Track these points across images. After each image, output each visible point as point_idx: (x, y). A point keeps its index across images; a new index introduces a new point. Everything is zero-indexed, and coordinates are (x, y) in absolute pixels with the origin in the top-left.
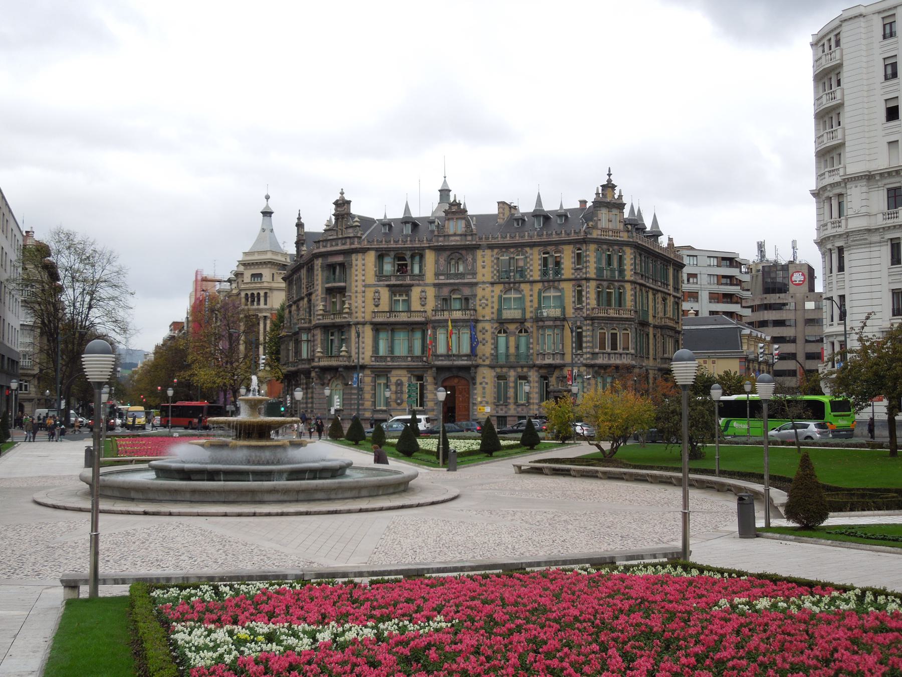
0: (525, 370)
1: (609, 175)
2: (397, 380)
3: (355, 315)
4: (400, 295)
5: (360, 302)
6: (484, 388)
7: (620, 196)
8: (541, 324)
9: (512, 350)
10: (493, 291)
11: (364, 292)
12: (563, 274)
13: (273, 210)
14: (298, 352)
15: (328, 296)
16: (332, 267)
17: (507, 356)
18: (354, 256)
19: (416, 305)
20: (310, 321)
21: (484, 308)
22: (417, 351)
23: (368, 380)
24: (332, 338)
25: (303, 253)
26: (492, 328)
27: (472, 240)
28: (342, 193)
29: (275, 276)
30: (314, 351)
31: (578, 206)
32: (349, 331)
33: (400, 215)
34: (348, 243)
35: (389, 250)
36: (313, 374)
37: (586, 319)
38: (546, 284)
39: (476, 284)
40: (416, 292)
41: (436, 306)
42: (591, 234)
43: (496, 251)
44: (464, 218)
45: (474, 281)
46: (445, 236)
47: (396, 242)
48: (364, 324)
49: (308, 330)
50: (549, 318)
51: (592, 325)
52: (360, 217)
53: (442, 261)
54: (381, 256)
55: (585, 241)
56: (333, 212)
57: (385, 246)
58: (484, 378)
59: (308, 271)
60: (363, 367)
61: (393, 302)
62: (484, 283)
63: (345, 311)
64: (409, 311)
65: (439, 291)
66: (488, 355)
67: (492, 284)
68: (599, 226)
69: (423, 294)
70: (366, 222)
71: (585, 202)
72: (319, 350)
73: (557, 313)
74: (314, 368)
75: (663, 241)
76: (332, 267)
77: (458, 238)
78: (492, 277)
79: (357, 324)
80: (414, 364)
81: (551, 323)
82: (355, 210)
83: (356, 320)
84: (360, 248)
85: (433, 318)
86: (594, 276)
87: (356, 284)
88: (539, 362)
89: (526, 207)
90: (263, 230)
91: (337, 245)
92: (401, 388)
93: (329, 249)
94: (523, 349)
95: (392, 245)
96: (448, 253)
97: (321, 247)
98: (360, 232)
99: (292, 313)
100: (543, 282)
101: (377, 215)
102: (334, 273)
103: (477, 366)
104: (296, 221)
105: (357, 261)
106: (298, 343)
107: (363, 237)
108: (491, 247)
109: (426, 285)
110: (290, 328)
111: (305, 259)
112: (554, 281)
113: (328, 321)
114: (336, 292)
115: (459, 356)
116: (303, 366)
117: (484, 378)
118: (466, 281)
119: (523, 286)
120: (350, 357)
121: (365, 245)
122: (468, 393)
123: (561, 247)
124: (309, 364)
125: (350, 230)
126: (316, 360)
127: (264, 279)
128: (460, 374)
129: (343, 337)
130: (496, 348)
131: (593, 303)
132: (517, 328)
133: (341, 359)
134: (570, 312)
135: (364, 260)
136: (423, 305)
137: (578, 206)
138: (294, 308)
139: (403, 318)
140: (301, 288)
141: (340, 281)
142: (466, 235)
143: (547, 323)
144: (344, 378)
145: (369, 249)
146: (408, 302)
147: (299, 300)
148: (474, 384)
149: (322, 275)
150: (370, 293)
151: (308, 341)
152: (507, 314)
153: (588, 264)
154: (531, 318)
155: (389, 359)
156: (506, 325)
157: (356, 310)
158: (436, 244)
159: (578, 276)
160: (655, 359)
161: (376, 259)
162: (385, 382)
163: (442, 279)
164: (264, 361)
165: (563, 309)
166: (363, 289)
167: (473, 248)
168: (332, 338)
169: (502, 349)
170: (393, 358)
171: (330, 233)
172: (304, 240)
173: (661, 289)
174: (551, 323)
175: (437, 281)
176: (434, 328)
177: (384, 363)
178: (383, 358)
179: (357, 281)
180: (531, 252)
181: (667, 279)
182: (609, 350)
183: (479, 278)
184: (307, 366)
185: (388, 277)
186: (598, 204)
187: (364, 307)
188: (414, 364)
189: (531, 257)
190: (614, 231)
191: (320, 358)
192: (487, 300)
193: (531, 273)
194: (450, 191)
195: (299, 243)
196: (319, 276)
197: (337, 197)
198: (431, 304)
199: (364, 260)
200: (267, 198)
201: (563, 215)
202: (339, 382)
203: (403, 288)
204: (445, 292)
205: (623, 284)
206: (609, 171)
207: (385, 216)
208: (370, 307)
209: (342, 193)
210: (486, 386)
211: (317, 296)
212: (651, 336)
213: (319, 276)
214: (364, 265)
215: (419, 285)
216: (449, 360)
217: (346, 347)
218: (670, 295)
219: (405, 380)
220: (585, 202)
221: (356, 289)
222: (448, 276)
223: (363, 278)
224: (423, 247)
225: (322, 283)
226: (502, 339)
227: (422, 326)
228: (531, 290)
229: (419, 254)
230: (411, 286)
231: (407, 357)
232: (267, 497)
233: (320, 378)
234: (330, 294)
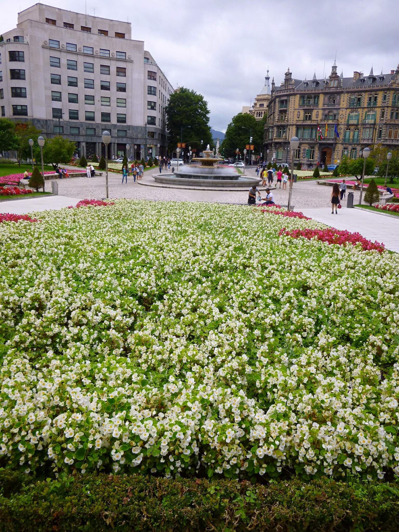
9: (351, 137)
16: (282, 102)
19: (314, 118)
31: (390, 73)
33: (311, 79)
39: (340, 109)
40: (314, 113)
48: (293, 125)
50: (368, 124)
52: (295, 80)
53: (326, 99)
55: (389, 89)
67: (346, 109)
70: (298, 82)
73: (372, 122)
79: (290, 125)
82: (293, 77)
86: (390, 105)
88: (362, 142)
94: (356, 137)
95: (307, 92)
96: (329, 95)
101: (303, 79)
103: (336, 144)
105: (292, 98)
108: (348, 92)
113: (279, 124)
114: (284, 112)
119: (359, 110)
121: (296, 92)
123: (378, 92)
130: (345, 136)
131: (389, 117)
134: (378, 121)
137: (390, 73)
139: (308, 123)
143: (367, 126)
145: (297, 94)
150: (296, 113)
152: (351, 122)
163: (326, 107)
167: (340, 93)
182: (392, 138)
183: (341, 106)
195: (272, 91)
196: (277, 104)
197: (287, 71)
198: (320, 117)
200: (268, 71)
201: (382, 78)
204: (327, 112)
208: (296, 118)
213: (277, 104)
222: (328, 105)
226: (348, 133)
227: (317, 126)
229: (316, 96)
233: (275, 146)
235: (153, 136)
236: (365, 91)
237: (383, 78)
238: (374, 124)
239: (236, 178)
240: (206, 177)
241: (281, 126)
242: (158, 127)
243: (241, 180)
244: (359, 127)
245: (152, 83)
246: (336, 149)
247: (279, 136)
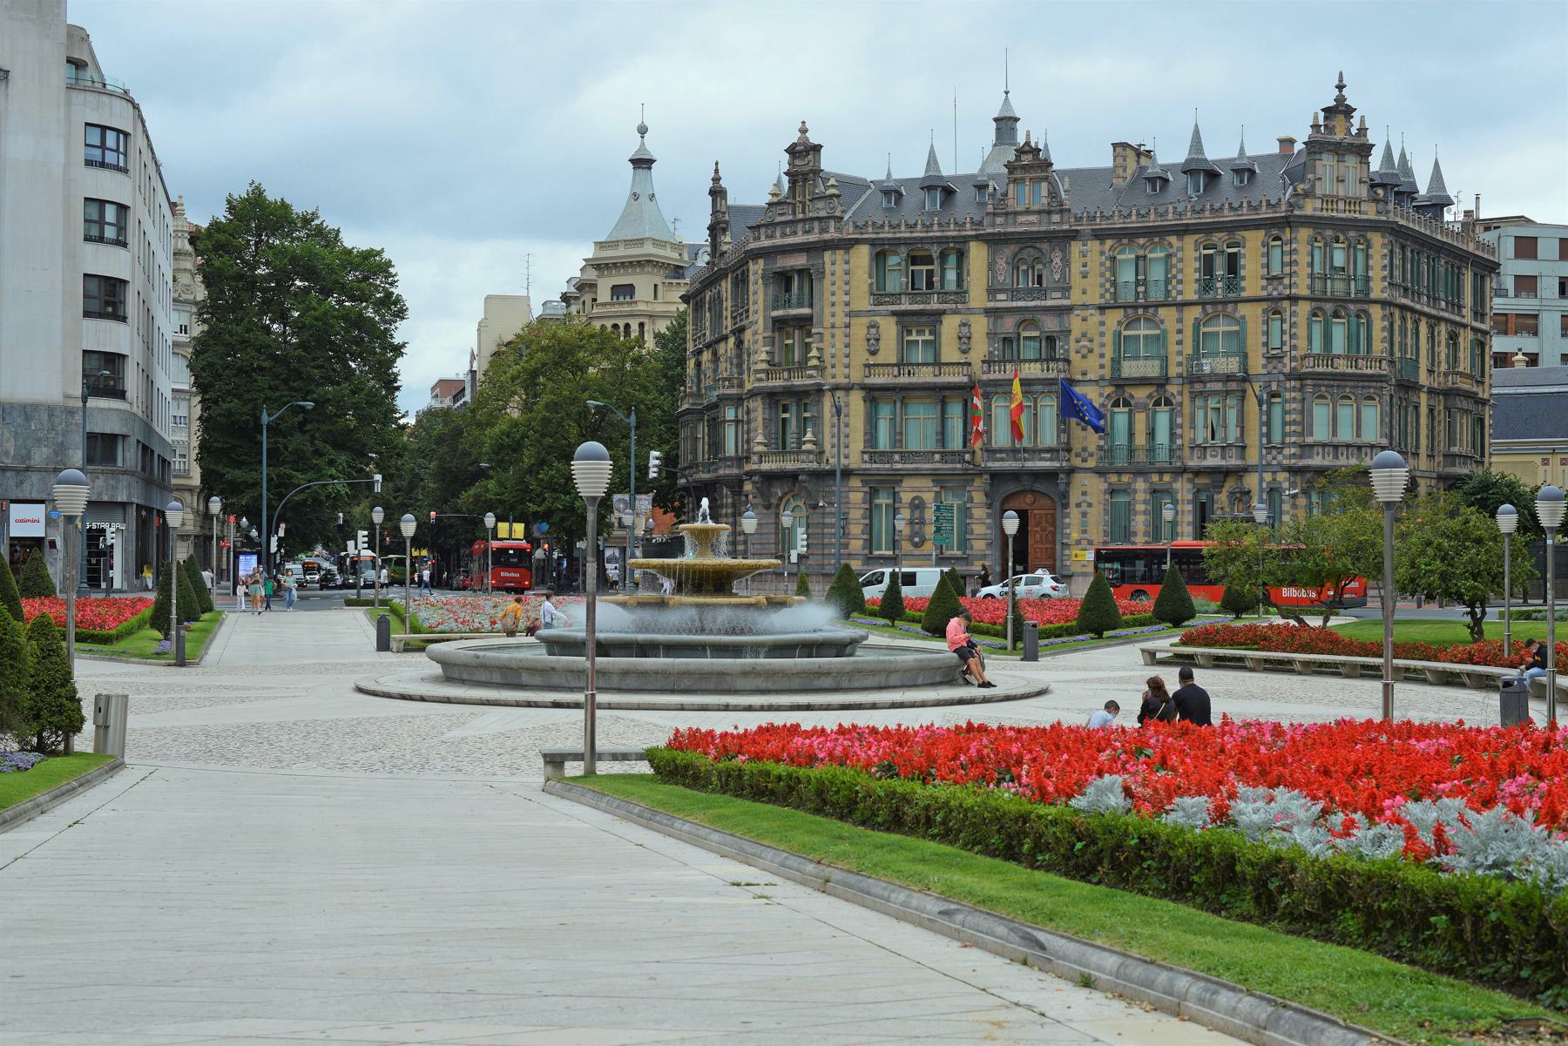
0: (1167, 478)
1: (1340, 87)
2: (914, 498)
3: (829, 371)
4: (920, 332)
5: (840, 345)
6: (1084, 515)
7: (1363, 131)
8: (1198, 387)
9: (1140, 439)
10: (1102, 324)
11: (848, 326)
12: (1243, 289)
13: (655, 156)
14: (716, 445)
15: (777, 334)
16: (784, 279)
17: (1131, 451)
18: (828, 256)
19: (950, 353)
20: (741, 385)
21: (1084, 357)
22: (956, 443)
23: (857, 497)
24: (785, 415)
25: (725, 248)
26: (1101, 395)
27: (1061, 223)
28: (804, 131)
29: (660, 288)
30: (748, 442)
31: (1275, 149)
32: (819, 402)
33: (920, 173)
34: (816, 230)
35: (897, 243)
36: (748, 487)
37: (1290, 376)
38: (1209, 308)
39: (1070, 309)
40: (950, 325)
41: (990, 353)
42: (1301, 208)
43: (1109, 243)
44: (1046, 179)
45: (1065, 302)
46: (1007, 214)
47: (911, 227)
48: (848, 389)
49: (738, 401)
50: (1215, 377)
51: (1301, 389)
52: (836, 176)
53: (1001, 264)
54: (880, 257)
55: (1288, 222)
56: (786, 167)
57: (890, 236)
58: (1084, 494)
59: (736, 284)
60: (847, 473)
61: (905, 346)
62: (1085, 306)
63: (810, 364)
64: (937, 363)
65: (995, 322)
66: (1092, 448)
67: (1102, 309)
68: (1318, 192)
69: (965, 330)
70: (853, 186)
71: (1291, 142)
72: (760, 439)
73: (1232, 365)
74: (750, 474)
76: (784, 279)
77: (1032, 218)
78: (1102, 296)
79: (835, 388)
80: (946, 466)
81: (1218, 386)
82: (829, 163)
83: (833, 381)
84: (840, 240)
85: (985, 377)
86: (1306, 292)
87: (833, 309)
88: (1194, 462)
90: (635, 196)
91: (795, 233)
92: (922, 513)
93: (778, 241)
95: (904, 234)
96: (1014, 248)
97: (763, 237)
98: (840, 208)
99: (703, 367)
100: (1203, 304)
102: (788, 289)
103: (1071, 471)
104: (710, 184)
106: (716, 425)
107: (846, 217)
108: (1100, 236)
109: (970, 311)
110: (699, 395)
111: (730, 260)
112: (1225, 303)
113: (777, 383)
115: (1035, 452)
116: (728, 471)
117: (1084, 494)
118: (1049, 303)
119: (1162, 312)
120: (822, 453)
121: (849, 232)
122: (1054, 524)
124: (740, 466)
125: (820, 204)
126: (755, 458)
127: (637, 297)
128: (1038, 487)
129: (807, 415)
132: (1150, 396)
133: (803, 457)
134: (1257, 364)
135: (847, 262)
136: (964, 352)
137: (1275, 149)
138: (706, 356)
139: (926, 376)
140: (721, 316)
141: (800, 305)
142: (1049, 213)
144: (809, 494)
145: (857, 242)
146: (934, 345)
147: (717, 342)
148: (1066, 506)
149: (766, 294)
150: (860, 328)
151: (737, 422)
152: (1130, 369)
153: (1294, 268)
154: (1180, 376)
155: (897, 457)
156: (1129, 390)
157: (834, 361)
158: (990, 230)
159: (1275, 293)
160: (1431, 456)
161: (871, 260)
162: (890, 501)
163: (1002, 301)
164: (657, 462)
166: (847, 320)
168: (785, 415)
170: (907, 456)
171: (779, 210)
172: (727, 223)
173: (1446, 315)
174: (1218, 386)
175: (991, 305)
176: (987, 396)
177: (887, 466)
178: (885, 456)
179: (833, 304)
180: (1180, 244)
181: (1458, 292)
183: (1076, 298)
184: (735, 471)
185: (896, 297)
186: (1315, 147)
187: (848, 356)
188: (946, 466)
189: (1180, 255)
190: (1349, 201)
191: (761, 455)
192: (1091, 341)
193: (1180, 287)
194: (1017, 120)
195: (715, 229)
196: (759, 294)
197: (794, 137)
198: (980, 349)
199: (847, 262)
200: (643, 130)
201: (1245, 172)
202: (801, 503)
203: (924, 319)
204: (1008, 325)
205: (1366, 306)
206: (1341, 79)
207: (889, 175)
208: (861, 356)
209: (804, 131)
210: (1088, 510)
211: (756, 333)
212: (1424, 410)
213: (759, 294)
214: (847, 273)
215: (956, 312)
216: (1016, 460)
217: (814, 434)
218: (1465, 326)
219: (928, 497)
220: (1291, 142)
221: (832, 320)
222: (1014, 293)
223: (846, 298)
224: (964, 237)
225: (765, 309)
227: (965, 391)
228: (1180, 321)
230: (940, 314)
231: (933, 453)
232: (741, 683)
234: (780, 329)
235: (110, 458)
237: (1252, 172)
239: (840, 648)
240: (736, 650)
241: (790, 392)
242: (135, 409)
243: (862, 657)
244: (1172, 389)
245: (110, 186)
246: (1074, 499)
247: (779, 445)
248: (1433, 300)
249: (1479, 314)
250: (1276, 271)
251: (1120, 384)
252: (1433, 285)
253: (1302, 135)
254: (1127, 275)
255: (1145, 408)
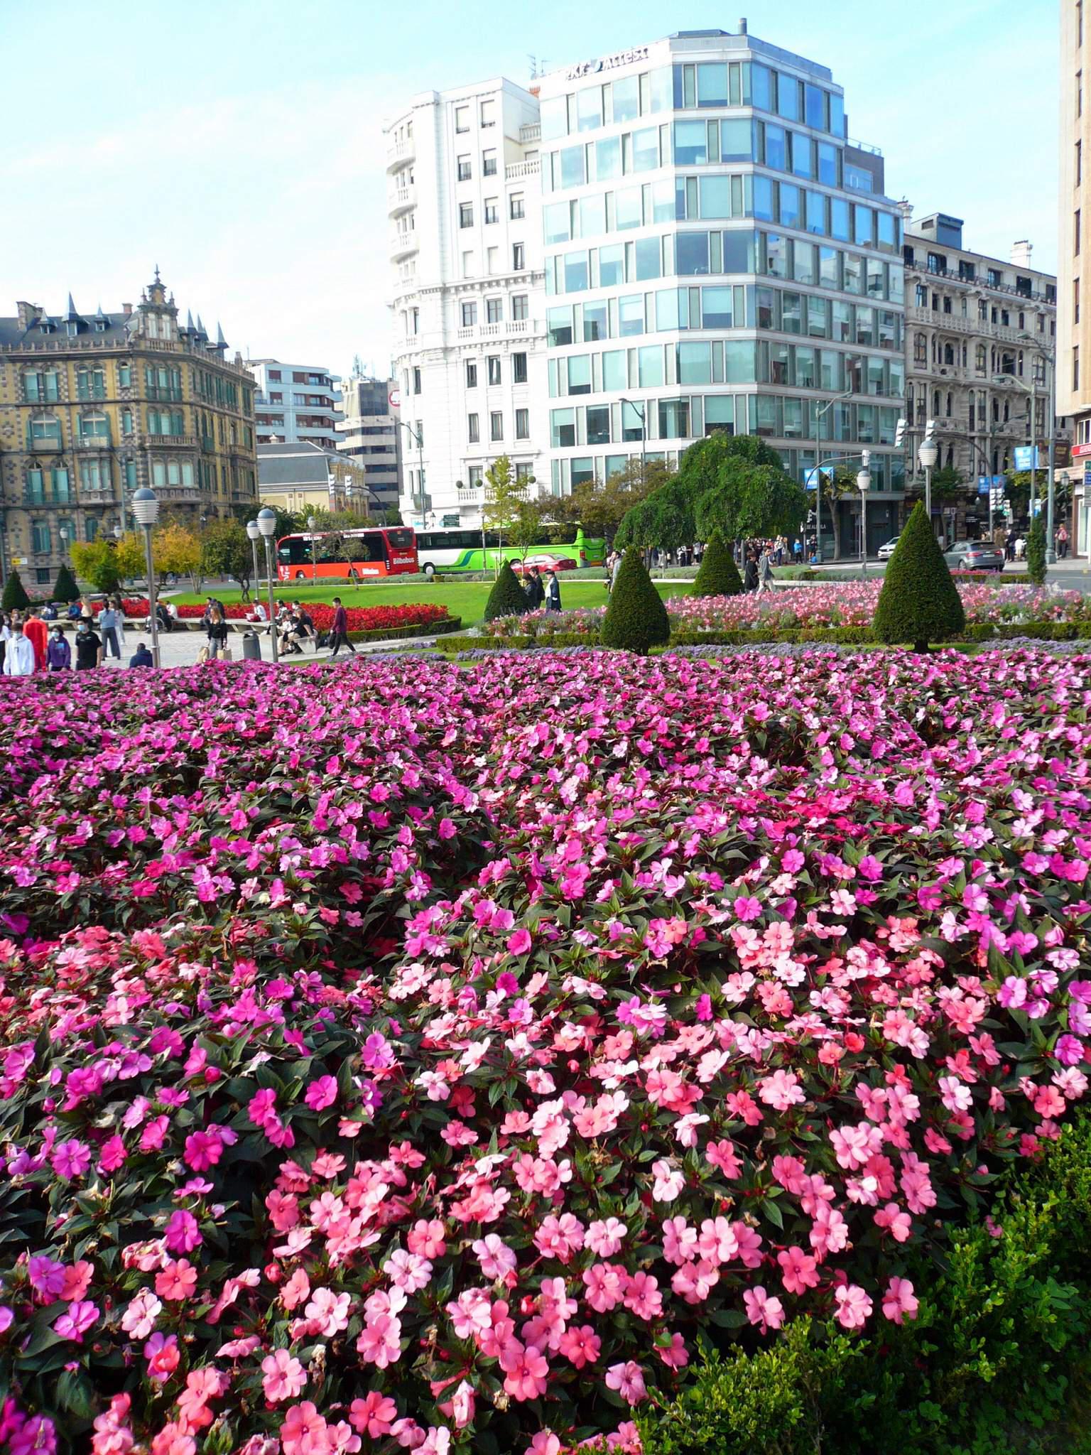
7: (172, 300)
8: (83, 456)
9: (49, 488)
17: (44, 496)
50: (92, 449)
67: (17, 406)
75: (229, 356)
81: (95, 455)
88: (83, 502)
89: (55, 309)
123: (101, 362)
137: (120, 310)
152: (41, 445)
156: (39, 459)
160: (225, 492)
165: (110, 436)
169: (37, 488)
174: (95, 455)
181: (235, 400)
186: (146, 308)
212: (219, 468)
226: (36, 476)
236: (68, 358)
238: (112, 449)
244: (67, 457)
246: (10, 526)
248: (221, 404)
249: (248, 413)
250: (127, 384)
251: (35, 454)
252: (219, 397)
253: (136, 302)
254: (33, 385)
255: (50, 468)
